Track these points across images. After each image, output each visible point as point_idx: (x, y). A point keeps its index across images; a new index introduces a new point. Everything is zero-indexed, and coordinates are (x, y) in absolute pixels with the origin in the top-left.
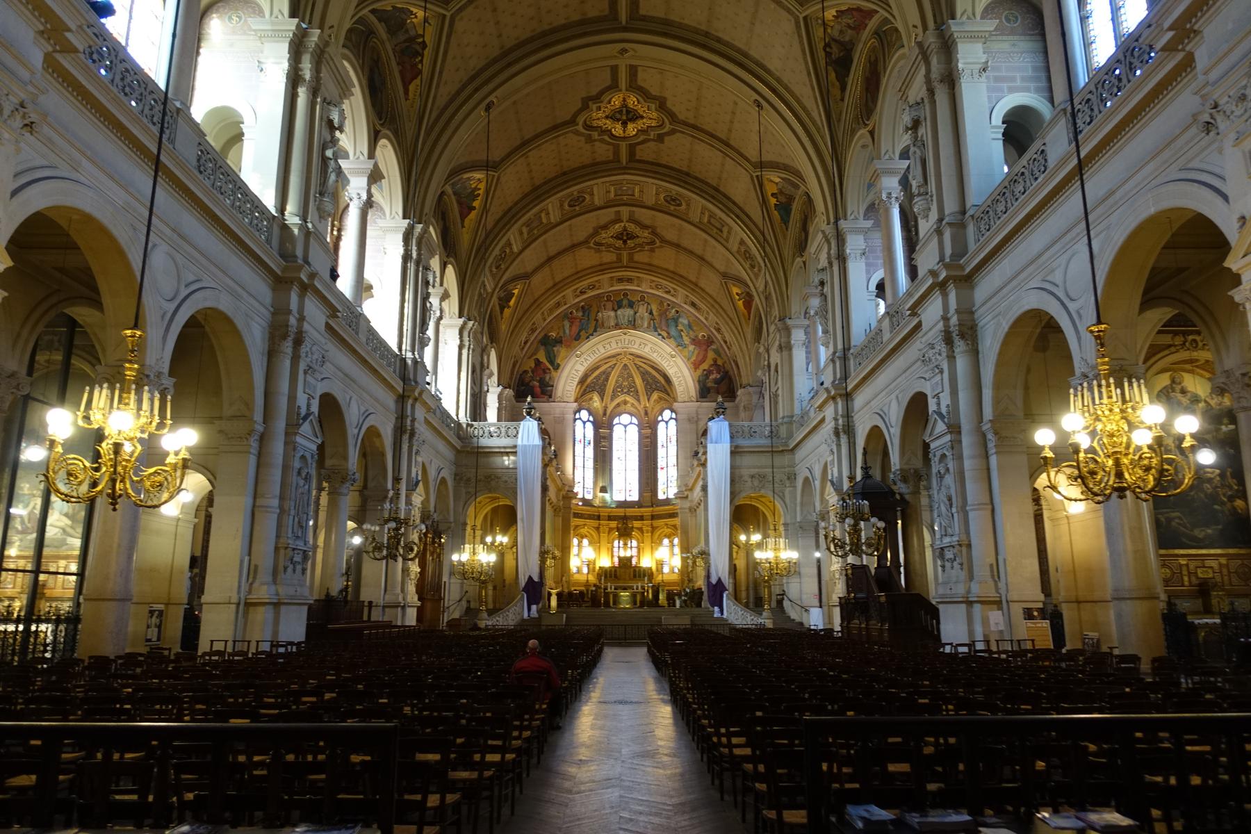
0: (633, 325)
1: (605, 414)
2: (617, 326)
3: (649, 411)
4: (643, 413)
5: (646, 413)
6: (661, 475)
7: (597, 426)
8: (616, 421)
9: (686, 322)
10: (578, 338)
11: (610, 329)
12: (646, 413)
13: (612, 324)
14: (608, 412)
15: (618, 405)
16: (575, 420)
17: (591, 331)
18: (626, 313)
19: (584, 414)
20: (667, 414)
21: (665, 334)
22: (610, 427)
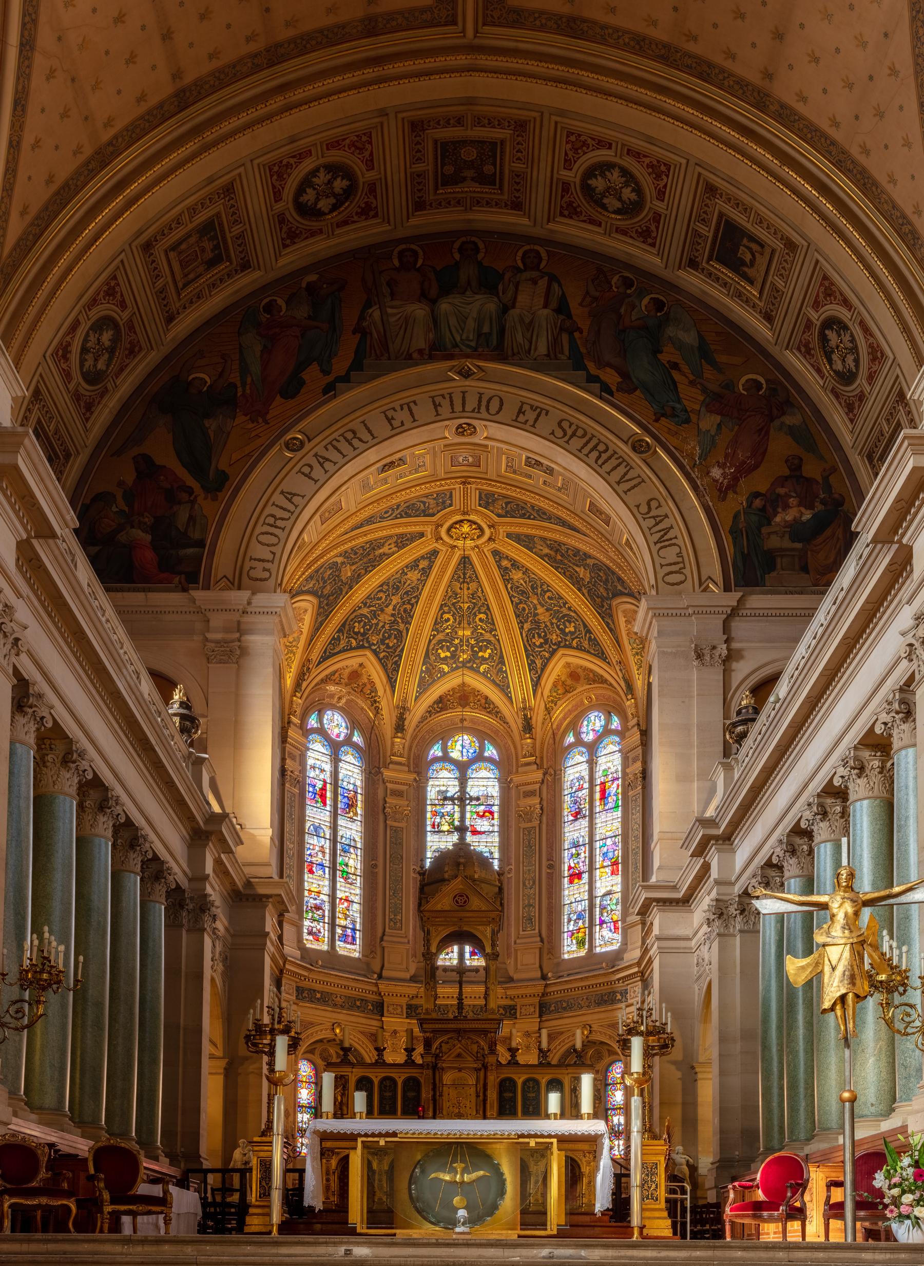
0: (496, 345)
1: (400, 727)
2: (437, 350)
3: (538, 719)
4: (516, 724)
5: (528, 727)
6: (573, 896)
7: (374, 761)
8: (436, 751)
9: (690, 338)
10: (292, 387)
11: (409, 359)
12: (528, 727)
13: (420, 341)
14: (413, 719)
15: (441, 704)
16: (306, 732)
17: (340, 366)
18: (470, 309)
19: (336, 724)
20: (594, 723)
21: (611, 377)
22: (419, 767)
